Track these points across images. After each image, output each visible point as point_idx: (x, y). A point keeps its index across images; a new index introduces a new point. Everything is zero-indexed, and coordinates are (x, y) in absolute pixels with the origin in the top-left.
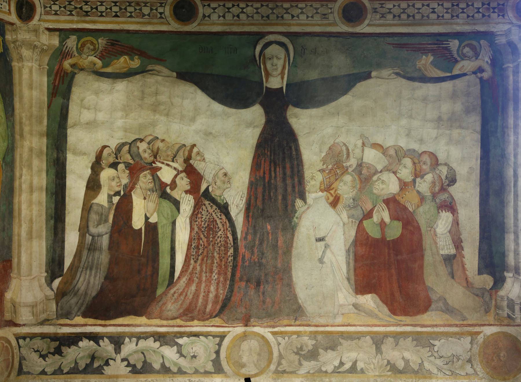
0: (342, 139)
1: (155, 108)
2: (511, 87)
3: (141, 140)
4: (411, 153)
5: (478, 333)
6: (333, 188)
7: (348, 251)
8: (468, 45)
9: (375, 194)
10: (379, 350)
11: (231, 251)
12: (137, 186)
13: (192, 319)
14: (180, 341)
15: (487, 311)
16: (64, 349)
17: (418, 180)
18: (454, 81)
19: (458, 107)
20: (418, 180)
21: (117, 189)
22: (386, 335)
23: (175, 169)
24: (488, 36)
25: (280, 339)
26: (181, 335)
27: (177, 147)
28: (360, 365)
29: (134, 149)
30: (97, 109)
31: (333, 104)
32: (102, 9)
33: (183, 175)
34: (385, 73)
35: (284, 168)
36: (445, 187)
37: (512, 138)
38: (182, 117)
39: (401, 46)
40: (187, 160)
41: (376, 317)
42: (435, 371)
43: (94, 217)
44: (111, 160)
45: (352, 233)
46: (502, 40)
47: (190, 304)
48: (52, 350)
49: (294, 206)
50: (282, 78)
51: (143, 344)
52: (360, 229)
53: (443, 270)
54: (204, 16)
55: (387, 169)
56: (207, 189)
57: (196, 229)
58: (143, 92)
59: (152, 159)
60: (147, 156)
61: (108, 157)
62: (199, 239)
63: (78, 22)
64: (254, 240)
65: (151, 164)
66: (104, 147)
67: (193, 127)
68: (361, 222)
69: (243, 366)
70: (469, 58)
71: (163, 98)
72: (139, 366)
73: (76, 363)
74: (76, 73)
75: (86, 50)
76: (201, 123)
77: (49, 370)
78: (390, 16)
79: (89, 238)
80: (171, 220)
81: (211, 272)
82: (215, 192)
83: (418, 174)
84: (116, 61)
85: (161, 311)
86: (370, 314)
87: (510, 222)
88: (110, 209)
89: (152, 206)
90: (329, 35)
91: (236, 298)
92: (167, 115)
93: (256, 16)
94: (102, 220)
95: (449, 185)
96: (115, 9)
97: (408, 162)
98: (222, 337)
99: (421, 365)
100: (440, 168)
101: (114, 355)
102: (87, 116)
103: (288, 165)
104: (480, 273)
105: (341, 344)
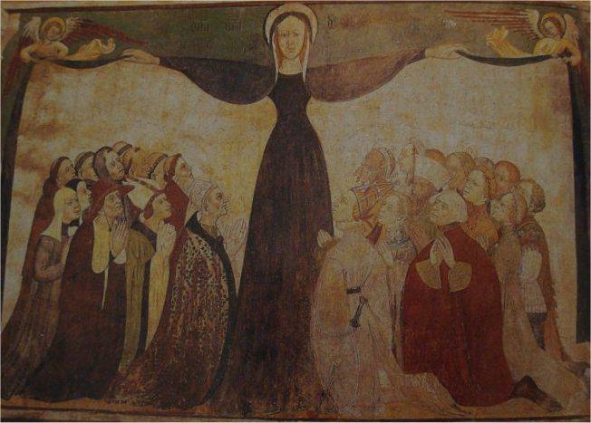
3: (110, 149)
6: (372, 215)
8: (551, 19)
9: (432, 223)
18: (537, 64)
21: (74, 216)
23: (152, 188)
27: (156, 158)
29: (100, 161)
33: (163, 196)
34: (445, 49)
36: (529, 213)
40: (168, 177)
43: (43, 255)
44: (70, 177)
50: (302, 61)
52: (412, 276)
56: (194, 216)
59: (122, 174)
60: (116, 171)
61: (66, 174)
65: (120, 182)
66: (62, 159)
68: (412, 265)
70: (554, 36)
74: (35, 63)
75: (50, 33)
80: (144, 261)
82: (206, 221)
84: (85, 46)
88: (63, 243)
95: (535, 211)
97: (478, 176)
100: (523, 185)
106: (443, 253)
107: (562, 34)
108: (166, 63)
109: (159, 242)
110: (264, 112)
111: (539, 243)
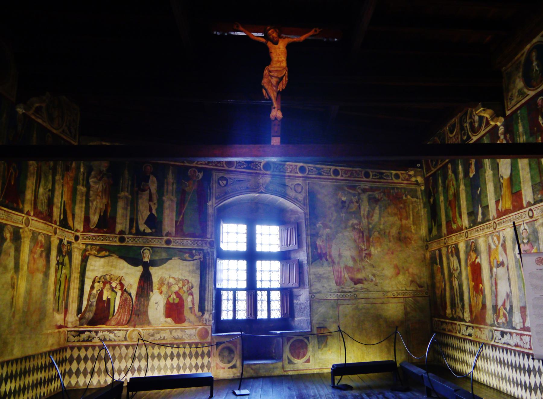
0: (164, 276)
1: (112, 266)
2: (208, 263)
3: (107, 275)
4: (182, 280)
5: (197, 328)
7: (164, 306)
10: (171, 333)
11: (131, 306)
12: (105, 288)
13: (119, 326)
14: (115, 332)
15: (200, 322)
16: (81, 335)
17: (184, 287)
19: (195, 268)
20: (184, 287)
21: (99, 289)
22: (173, 329)
24: (202, 250)
25: (144, 331)
26: (115, 330)
27: (117, 277)
28: (166, 338)
29: (105, 277)
30: (95, 266)
31: (162, 266)
32: (98, 238)
34: (176, 258)
35: (147, 283)
37: (208, 276)
38: (119, 269)
39: (181, 251)
40: (120, 281)
41: (171, 324)
42: (186, 338)
43: (92, 297)
44: (98, 280)
45: (165, 301)
46: (206, 251)
47: (119, 321)
48: (77, 335)
49: (149, 294)
51: (104, 333)
52: (168, 300)
53: (189, 311)
54: (127, 241)
55: (175, 284)
56: (125, 289)
57: (122, 300)
58: (109, 262)
59: (110, 280)
60: (108, 279)
61: (97, 279)
62: (122, 303)
63: (91, 242)
64: (138, 303)
66: (96, 277)
67: (122, 272)
68: (168, 298)
69: (133, 339)
70: (198, 255)
71: (114, 263)
72: (103, 339)
73: (84, 339)
76: (125, 270)
77: (76, 341)
78: (178, 244)
79: (90, 303)
81: (125, 312)
83: (184, 285)
85: (110, 323)
86: (169, 323)
87: (207, 298)
89: (109, 293)
90: (161, 248)
91: (132, 319)
92: (115, 268)
93: (142, 242)
94: (94, 297)
96: (102, 239)
97: (181, 282)
98: (127, 331)
99: (182, 337)
101: (95, 336)
102: (92, 268)
103: (149, 283)
104: (199, 311)
105: (161, 332)
106: (174, 296)
107: (200, 255)
108: (121, 257)
109: (118, 294)
110: (140, 269)
111: (191, 294)
